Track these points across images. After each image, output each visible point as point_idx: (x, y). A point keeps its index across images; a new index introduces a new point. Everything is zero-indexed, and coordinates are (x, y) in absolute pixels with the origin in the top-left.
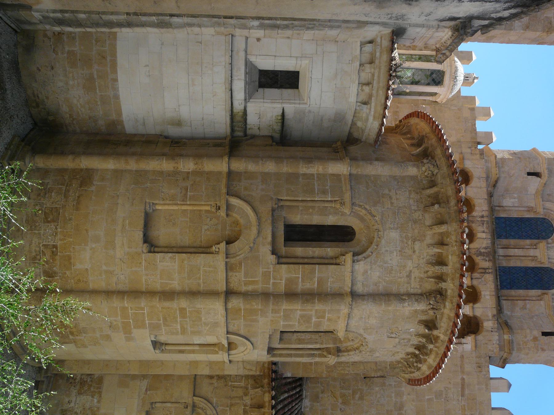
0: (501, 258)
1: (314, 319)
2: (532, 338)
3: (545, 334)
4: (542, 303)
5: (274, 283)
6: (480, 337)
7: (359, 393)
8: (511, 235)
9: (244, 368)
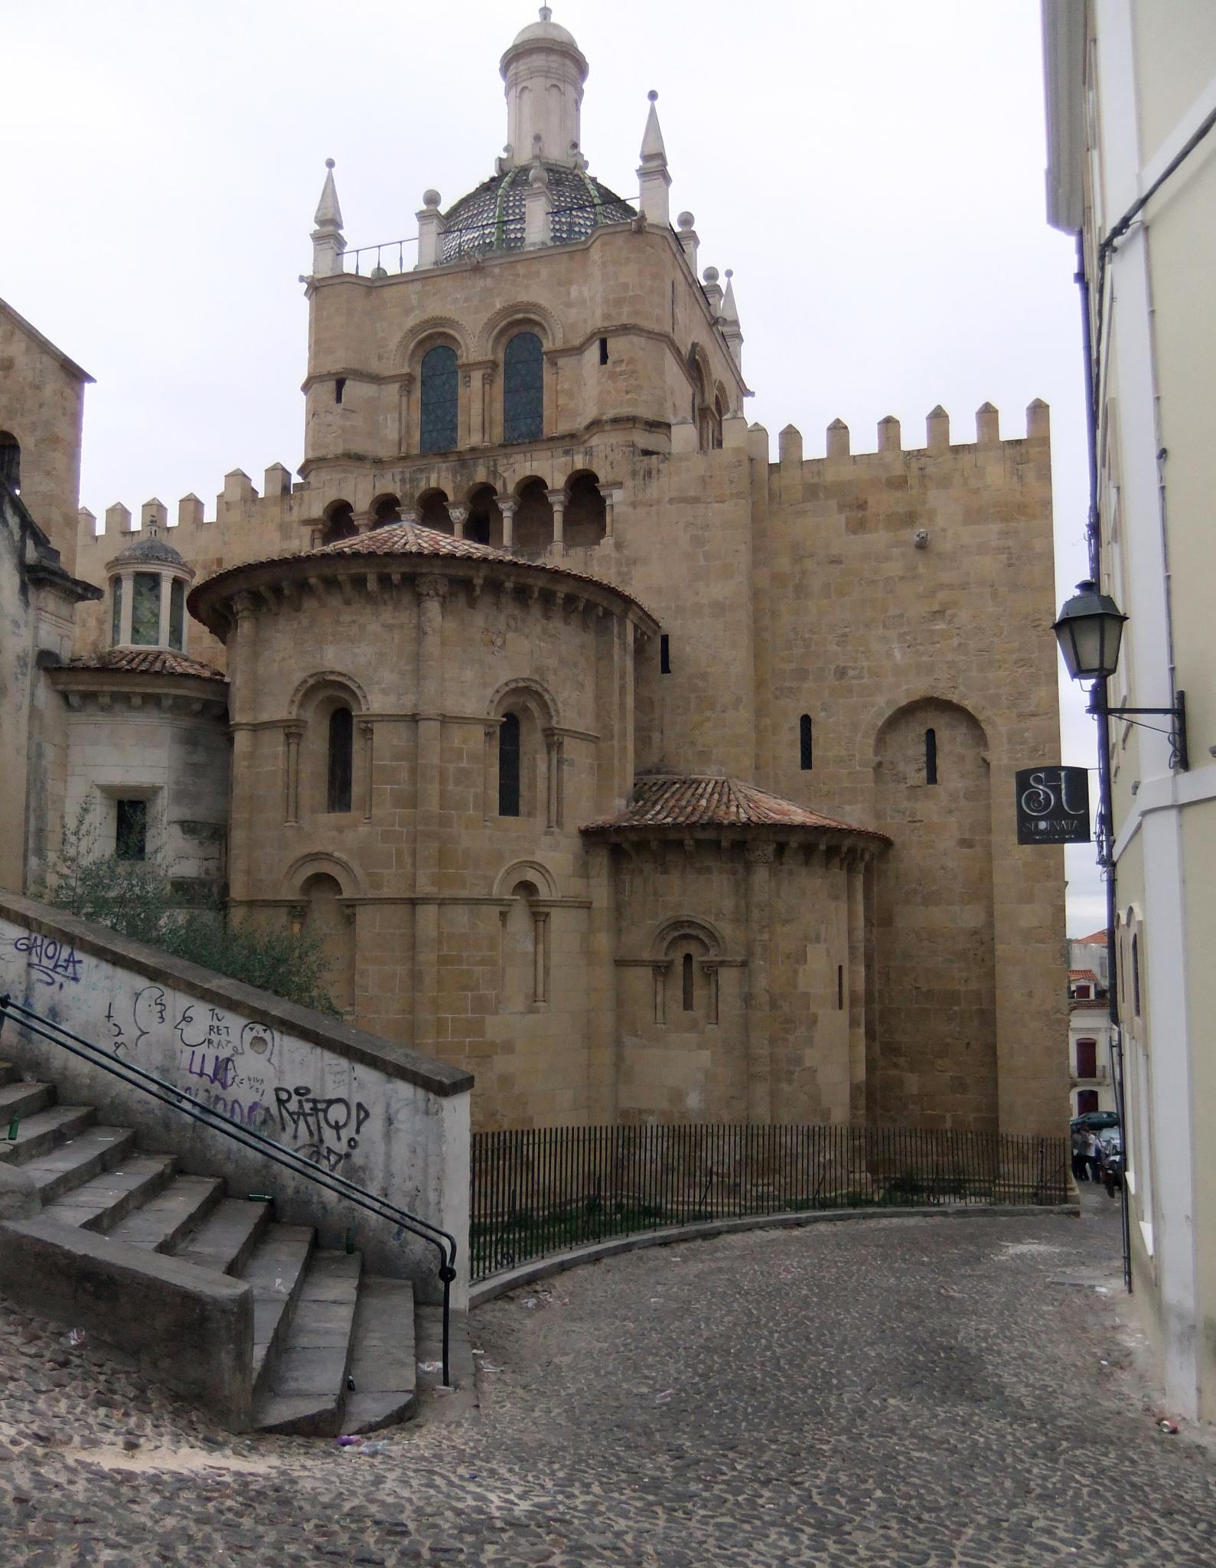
0: (487, 438)
1: (464, 764)
2: (610, 382)
3: (604, 358)
4: (561, 362)
5: (399, 826)
6: (603, 475)
7: (696, 681)
8: (451, 421)
9: (598, 875)
